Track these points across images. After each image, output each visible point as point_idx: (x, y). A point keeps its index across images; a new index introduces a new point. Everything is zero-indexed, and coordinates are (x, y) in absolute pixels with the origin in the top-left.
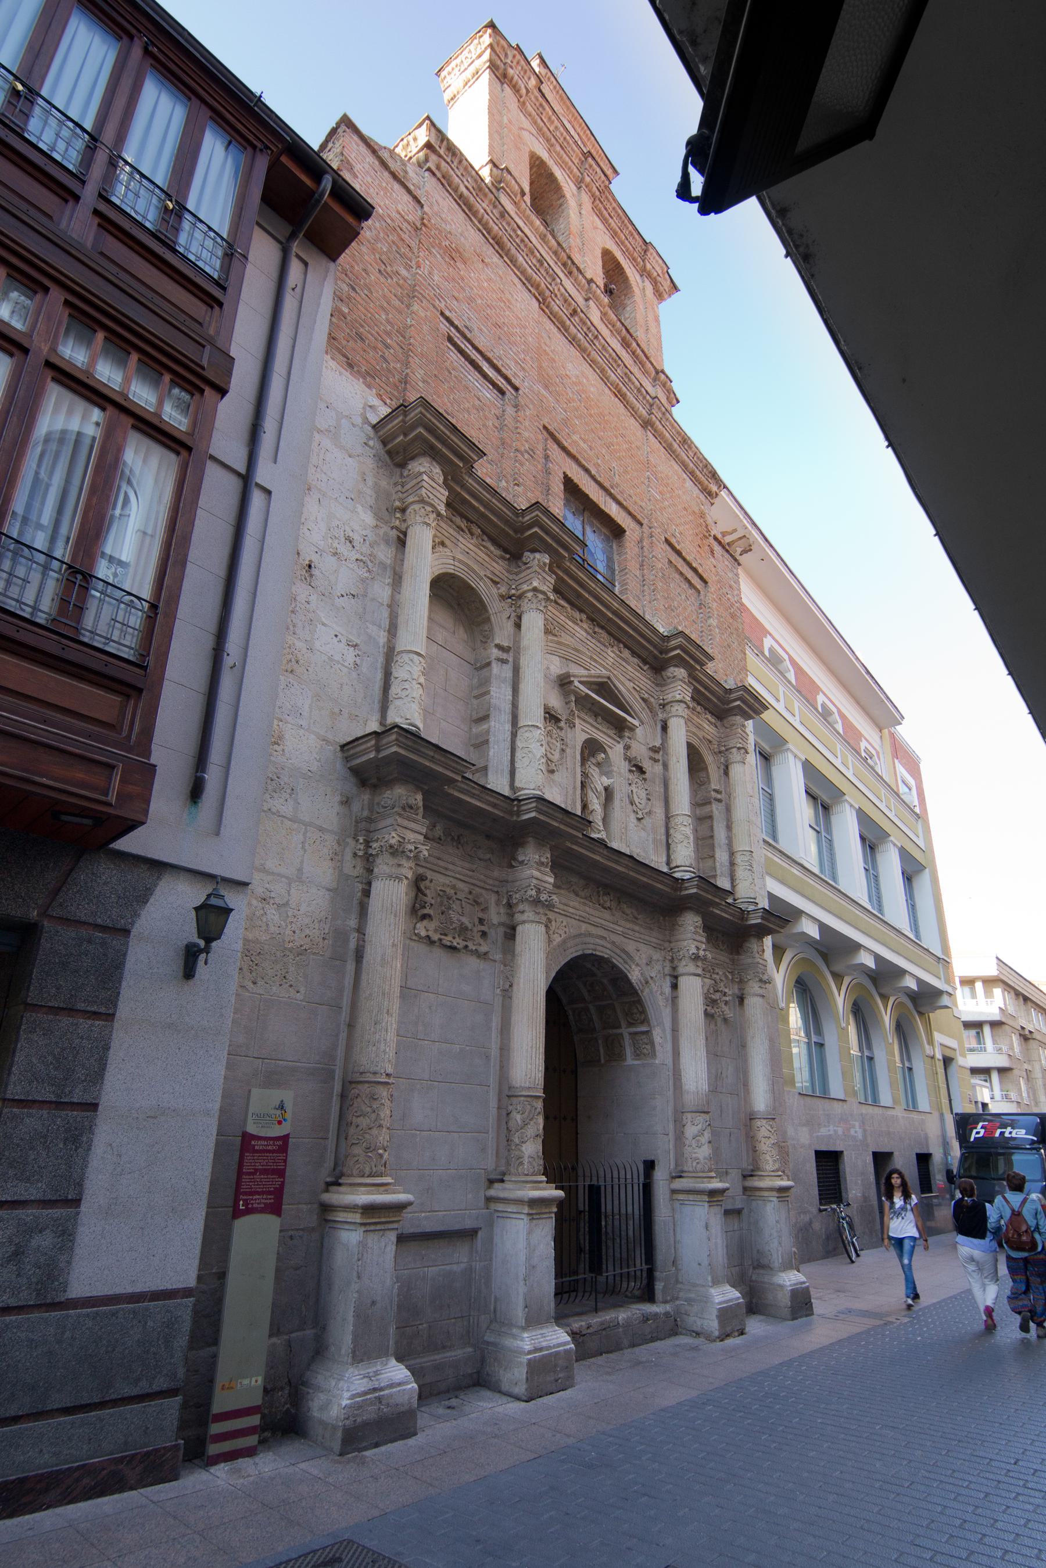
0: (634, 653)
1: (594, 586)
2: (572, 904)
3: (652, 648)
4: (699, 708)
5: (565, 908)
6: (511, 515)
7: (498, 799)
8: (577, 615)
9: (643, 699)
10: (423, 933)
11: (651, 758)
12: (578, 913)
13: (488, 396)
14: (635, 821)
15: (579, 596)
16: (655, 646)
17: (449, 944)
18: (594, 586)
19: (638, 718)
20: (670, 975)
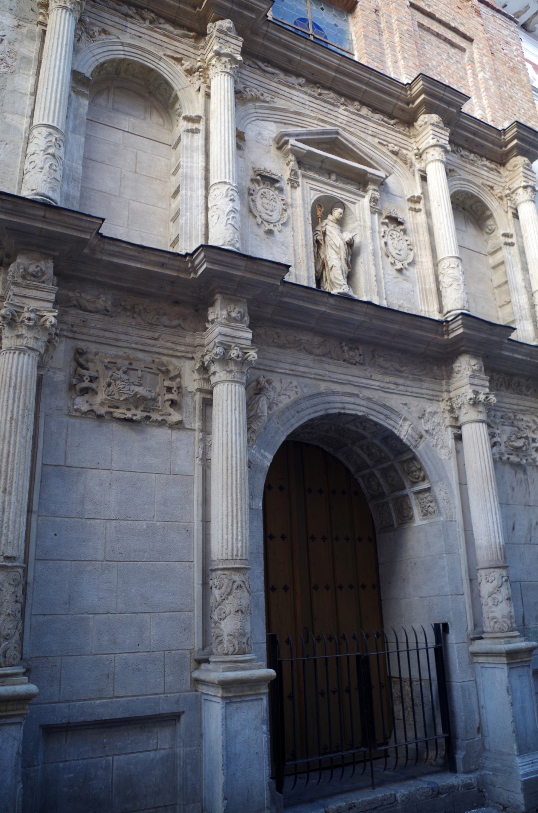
0: (375, 110)
1: (303, 46)
2: (302, 362)
4: (472, 156)
5: (293, 367)
7: (164, 257)
8: (292, 79)
9: (393, 152)
10: (85, 408)
11: (411, 209)
14: (395, 273)
15: (290, 60)
17: (122, 416)
18: (303, 46)
19: (383, 168)
20: (451, 426)
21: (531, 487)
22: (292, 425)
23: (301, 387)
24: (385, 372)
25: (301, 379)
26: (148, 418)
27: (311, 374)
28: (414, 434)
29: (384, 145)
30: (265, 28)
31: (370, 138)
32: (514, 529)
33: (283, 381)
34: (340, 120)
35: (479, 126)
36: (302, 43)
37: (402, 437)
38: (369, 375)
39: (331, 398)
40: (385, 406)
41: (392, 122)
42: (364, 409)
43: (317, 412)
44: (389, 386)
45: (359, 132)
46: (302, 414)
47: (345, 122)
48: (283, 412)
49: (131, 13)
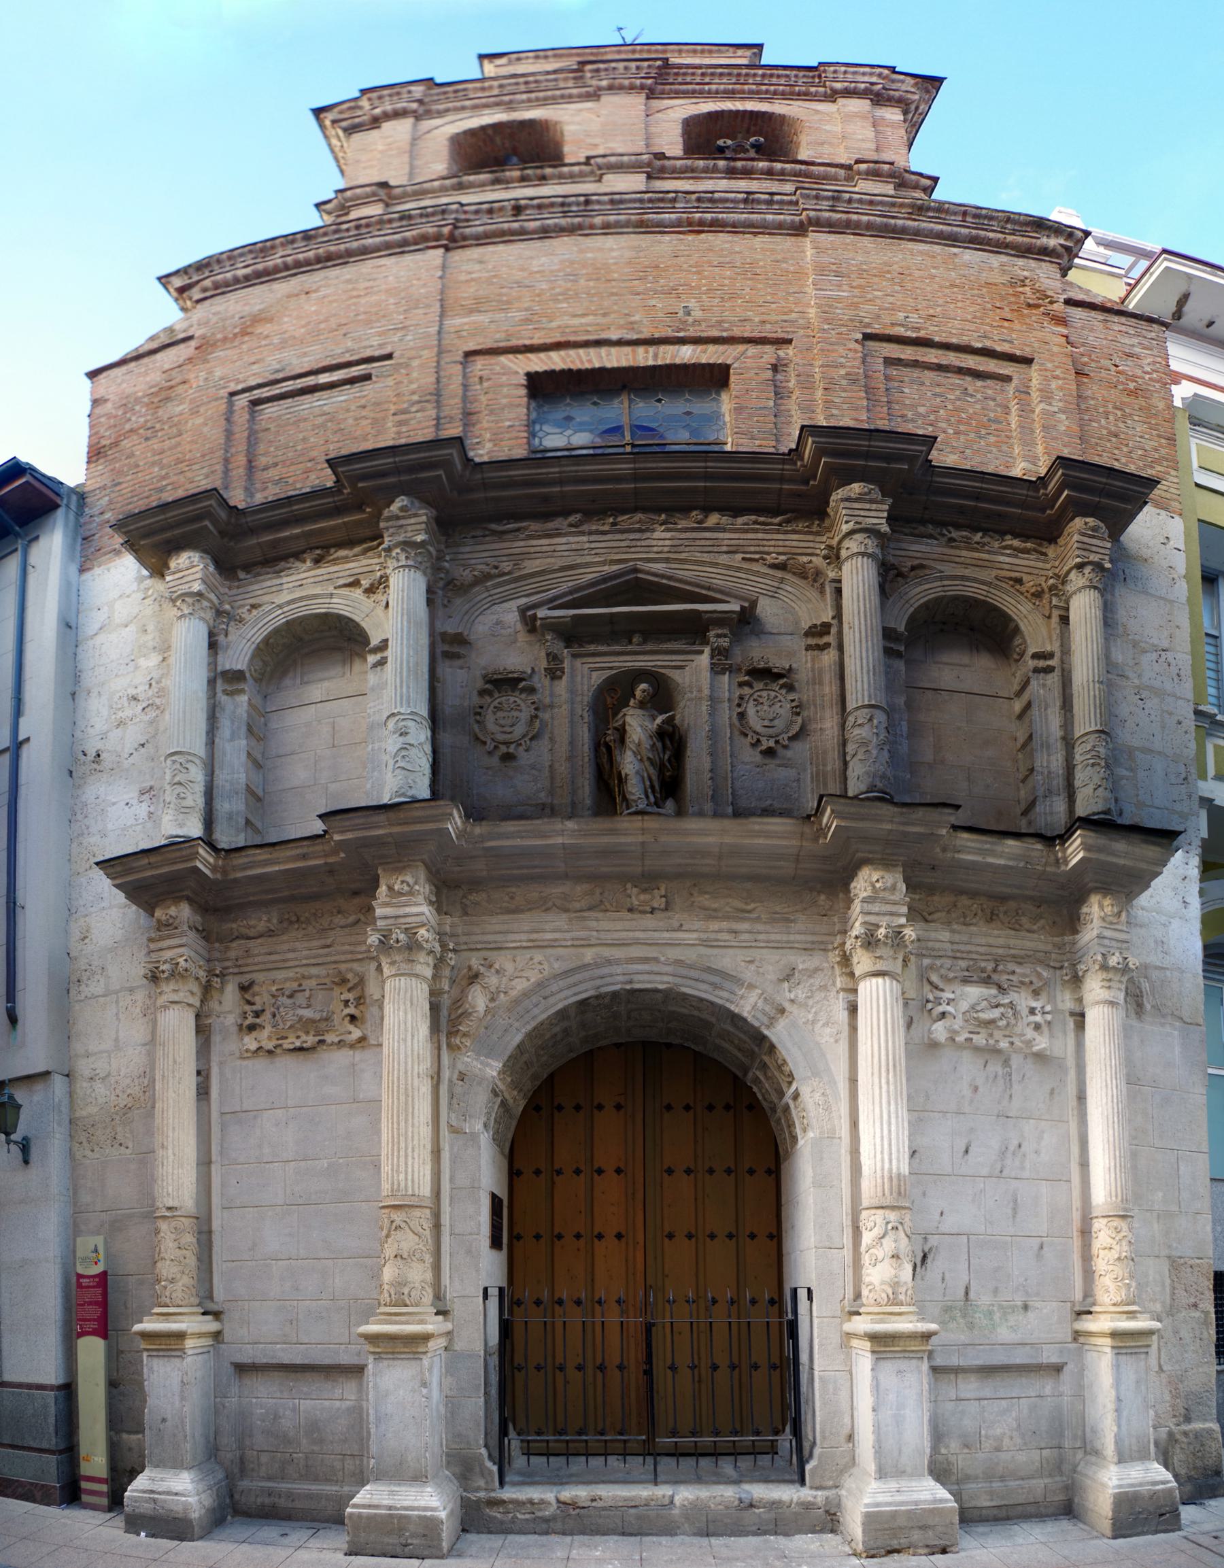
5: (535, 936)
12: (568, 936)
22: (534, 1018)
23: (548, 961)
24: (712, 915)
25: (549, 951)
27: (565, 940)
28: (767, 1008)
33: (518, 959)
37: (745, 1014)
38: (676, 924)
39: (606, 970)
42: (666, 978)
43: (580, 993)
44: (720, 936)
46: (552, 1000)
48: (517, 1002)
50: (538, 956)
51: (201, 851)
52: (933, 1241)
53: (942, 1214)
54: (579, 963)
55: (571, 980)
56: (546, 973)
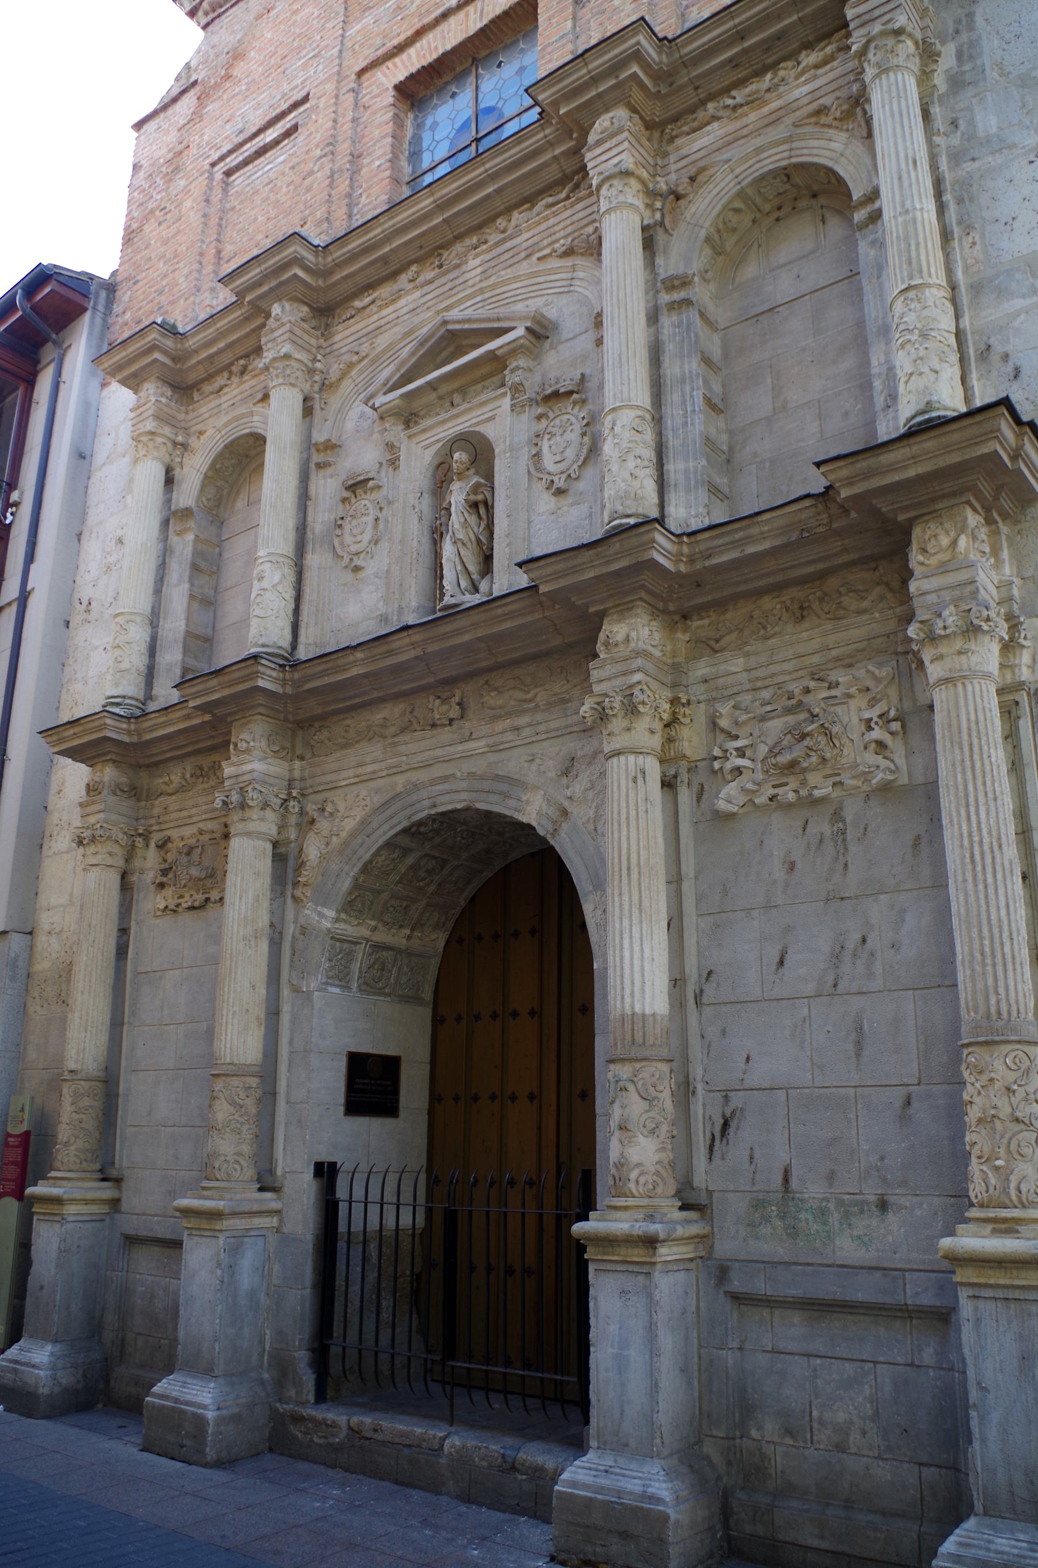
1: (379, 230)
3: (548, 156)
5: (360, 771)
6: (239, 313)
12: (383, 765)
13: (281, 159)
15: (384, 260)
16: (551, 144)
18: (379, 230)
21: (853, 848)
26: (207, 900)
29: (550, 255)
30: (330, 259)
31: (524, 268)
32: (781, 963)
34: (470, 283)
35: (732, 18)
36: (376, 228)
37: (534, 824)
39: (414, 797)
40: (498, 778)
41: (563, 195)
45: (503, 273)
46: (374, 837)
47: (478, 279)
48: (346, 844)
49: (223, 383)
50: (363, 790)
51: (109, 721)
52: (737, 1100)
53: (748, 1059)
54: (393, 793)
55: (389, 812)
56: (367, 809)
